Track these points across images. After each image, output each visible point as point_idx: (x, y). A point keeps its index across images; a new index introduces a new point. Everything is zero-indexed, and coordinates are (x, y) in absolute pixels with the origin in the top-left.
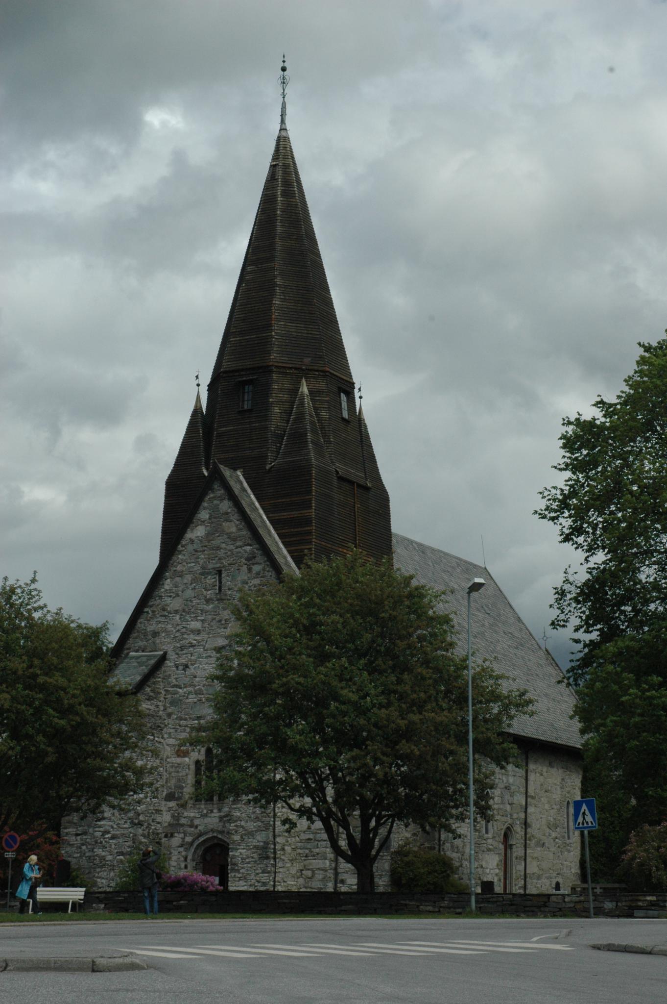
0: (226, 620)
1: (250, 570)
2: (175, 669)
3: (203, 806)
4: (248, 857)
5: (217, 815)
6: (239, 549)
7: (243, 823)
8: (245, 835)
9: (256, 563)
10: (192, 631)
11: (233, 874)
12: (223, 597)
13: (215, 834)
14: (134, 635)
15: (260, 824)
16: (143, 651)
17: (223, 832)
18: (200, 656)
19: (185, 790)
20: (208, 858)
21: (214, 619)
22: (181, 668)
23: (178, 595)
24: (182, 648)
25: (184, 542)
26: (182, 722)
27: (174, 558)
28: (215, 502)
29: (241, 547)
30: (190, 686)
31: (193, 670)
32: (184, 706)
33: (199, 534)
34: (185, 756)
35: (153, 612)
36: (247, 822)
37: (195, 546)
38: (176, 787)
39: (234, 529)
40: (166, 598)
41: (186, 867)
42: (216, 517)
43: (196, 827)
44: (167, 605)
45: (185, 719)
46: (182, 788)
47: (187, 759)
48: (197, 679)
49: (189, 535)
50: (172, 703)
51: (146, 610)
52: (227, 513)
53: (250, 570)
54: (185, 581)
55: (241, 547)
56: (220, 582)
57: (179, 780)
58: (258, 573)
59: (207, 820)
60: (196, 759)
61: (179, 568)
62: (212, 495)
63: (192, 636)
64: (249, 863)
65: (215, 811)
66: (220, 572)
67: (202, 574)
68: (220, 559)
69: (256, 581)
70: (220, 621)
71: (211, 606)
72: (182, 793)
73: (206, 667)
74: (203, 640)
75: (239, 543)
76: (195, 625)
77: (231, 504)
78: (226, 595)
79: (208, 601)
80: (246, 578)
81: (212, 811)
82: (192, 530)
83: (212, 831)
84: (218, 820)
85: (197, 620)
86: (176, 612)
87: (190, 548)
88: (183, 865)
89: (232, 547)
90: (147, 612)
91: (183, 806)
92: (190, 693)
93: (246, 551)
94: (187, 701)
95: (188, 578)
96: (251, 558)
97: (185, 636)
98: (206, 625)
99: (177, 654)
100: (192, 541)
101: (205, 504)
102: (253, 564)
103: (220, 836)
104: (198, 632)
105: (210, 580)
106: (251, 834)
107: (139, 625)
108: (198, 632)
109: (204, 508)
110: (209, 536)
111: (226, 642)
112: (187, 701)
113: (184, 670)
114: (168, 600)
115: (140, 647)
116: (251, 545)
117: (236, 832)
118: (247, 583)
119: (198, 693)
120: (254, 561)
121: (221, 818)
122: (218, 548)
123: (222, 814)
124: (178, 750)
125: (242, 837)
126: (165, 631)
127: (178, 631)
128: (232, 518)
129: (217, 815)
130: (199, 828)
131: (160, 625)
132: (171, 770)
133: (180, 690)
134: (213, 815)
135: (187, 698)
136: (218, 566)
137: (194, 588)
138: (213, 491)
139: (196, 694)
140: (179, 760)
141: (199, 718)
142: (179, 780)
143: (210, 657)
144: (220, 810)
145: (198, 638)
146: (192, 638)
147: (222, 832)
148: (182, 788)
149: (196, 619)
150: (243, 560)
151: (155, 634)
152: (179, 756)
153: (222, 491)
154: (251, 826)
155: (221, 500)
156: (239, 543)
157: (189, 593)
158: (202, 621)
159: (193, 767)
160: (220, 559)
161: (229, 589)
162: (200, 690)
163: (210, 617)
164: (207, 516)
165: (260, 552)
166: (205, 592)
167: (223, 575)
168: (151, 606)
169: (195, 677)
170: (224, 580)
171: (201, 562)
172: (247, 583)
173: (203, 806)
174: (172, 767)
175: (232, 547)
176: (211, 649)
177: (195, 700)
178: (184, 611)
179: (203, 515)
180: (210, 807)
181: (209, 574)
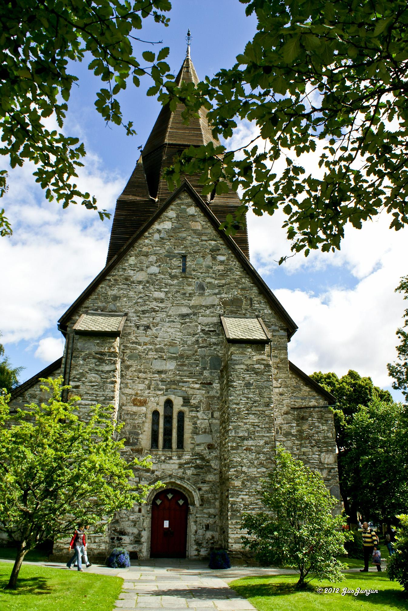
0: (190, 294)
1: (214, 258)
2: (136, 329)
3: (160, 453)
4: (251, 504)
5: (177, 461)
6: (204, 242)
7: (245, 469)
8: (248, 481)
9: (219, 255)
10: (156, 299)
11: (234, 521)
12: (188, 276)
13: (173, 480)
14: (93, 297)
15: (264, 470)
16: (102, 311)
17: (184, 478)
18: (162, 320)
19: (141, 436)
20: (159, 502)
21: (177, 292)
22: (142, 328)
23: (142, 270)
24: (144, 312)
25: (151, 231)
26: (140, 375)
27: (140, 241)
28: (182, 207)
29: (206, 241)
30: (150, 344)
31: (154, 331)
32: (144, 361)
33: (166, 227)
34: (143, 406)
35: (115, 280)
36: (249, 467)
37: (162, 235)
38: (130, 433)
39: (200, 228)
40: (129, 271)
41: (140, 511)
42: (181, 216)
43: (153, 472)
44: (130, 276)
45: (145, 372)
46: (138, 434)
47: (144, 408)
48: (158, 339)
49: (156, 226)
50: (130, 358)
51: (108, 278)
52: (193, 216)
53: (214, 258)
54: (150, 259)
55: (206, 241)
56: (184, 264)
57: (134, 427)
58: (222, 262)
59: (163, 466)
60: (154, 409)
61: (145, 249)
62: (179, 202)
63: (154, 303)
64: (253, 509)
65: (174, 458)
66: (184, 257)
67: (166, 256)
68: (185, 247)
69: (221, 268)
70: (185, 294)
71: (176, 281)
72: (137, 439)
73: (169, 330)
74: (166, 308)
75: (204, 238)
76: (162, 295)
77: (198, 209)
78: (191, 275)
79: (173, 277)
80: (211, 264)
81: (170, 458)
82: (159, 224)
83: (170, 476)
84: (177, 467)
85: (161, 291)
86: (140, 282)
87: (157, 236)
88: (137, 509)
89: (198, 240)
90: (110, 280)
91: (139, 452)
92: (151, 349)
93: (210, 245)
94: (147, 357)
95: (153, 258)
96: (215, 251)
97: (147, 303)
98: (169, 295)
99: (139, 316)
100: (159, 231)
101: (172, 207)
102: (218, 255)
103: (178, 482)
104: (162, 301)
105: (177, 262)
106: (254, 479)
107: (99, 289)
108: (162, 301)
109: (172, 210)
110: (174, 229)
111: (190, 311)
112: (147, 357)
113: (145, 330)
114: (131, 273)
115: (99, 307)
116: (215, 241)
117: (237, 477)
118: (212, 268)
119: (161, 350)
120: (218, 252)
121: (181, 466)
122: (184, 239)
123: (182, 461)
124: (134, 400)
125: (243, 483)
126: (127, 296)
127: (141, 297)
128: (198, 219)
129: (177, 461)
130: (156, 473)
131: (122, 292)
132: (126, 417)
133: (140, 347)
134: (171, 461)
135: (147, 354)
136: (184, 252)
137: (160, 266)
138: (180, 199)
139: (156, 352)
140: (135, 409)
141: (160, 372)
142: (134, 427)
143: (174, 322)
144: (179, 458)
145: (160, 305)
146: (154, 304)
147: (182, 479)
148: (138, 434)
149: (160, 290)
150: (208, 251)
151: (116, 298)
152: (135, 405)
153: (190, 200)
154: (253, 472)
155: (189, 206)
156: (204, 238)
157: (154, 269)
158: (166, 293)
159: (150, 416)
160: (185, 247)
161: (194, 270)
162: (162, 348)
163: (175, 290)
164: (175, 216)
165: (224, 247)
166: (169, 271)
167: (188, 260)
168: (113, 276)
169: (157, 337)
170: (188, 264)
171: (167, 248)
172: (212, 268)
173: (160, 453)
174: (127, 414)
175: (198, 240)
176: (175, 315)
177: (156, 357)
178: (148, 282)
179: (171, 213)
180: (169, 454)
181: (174, 257)
